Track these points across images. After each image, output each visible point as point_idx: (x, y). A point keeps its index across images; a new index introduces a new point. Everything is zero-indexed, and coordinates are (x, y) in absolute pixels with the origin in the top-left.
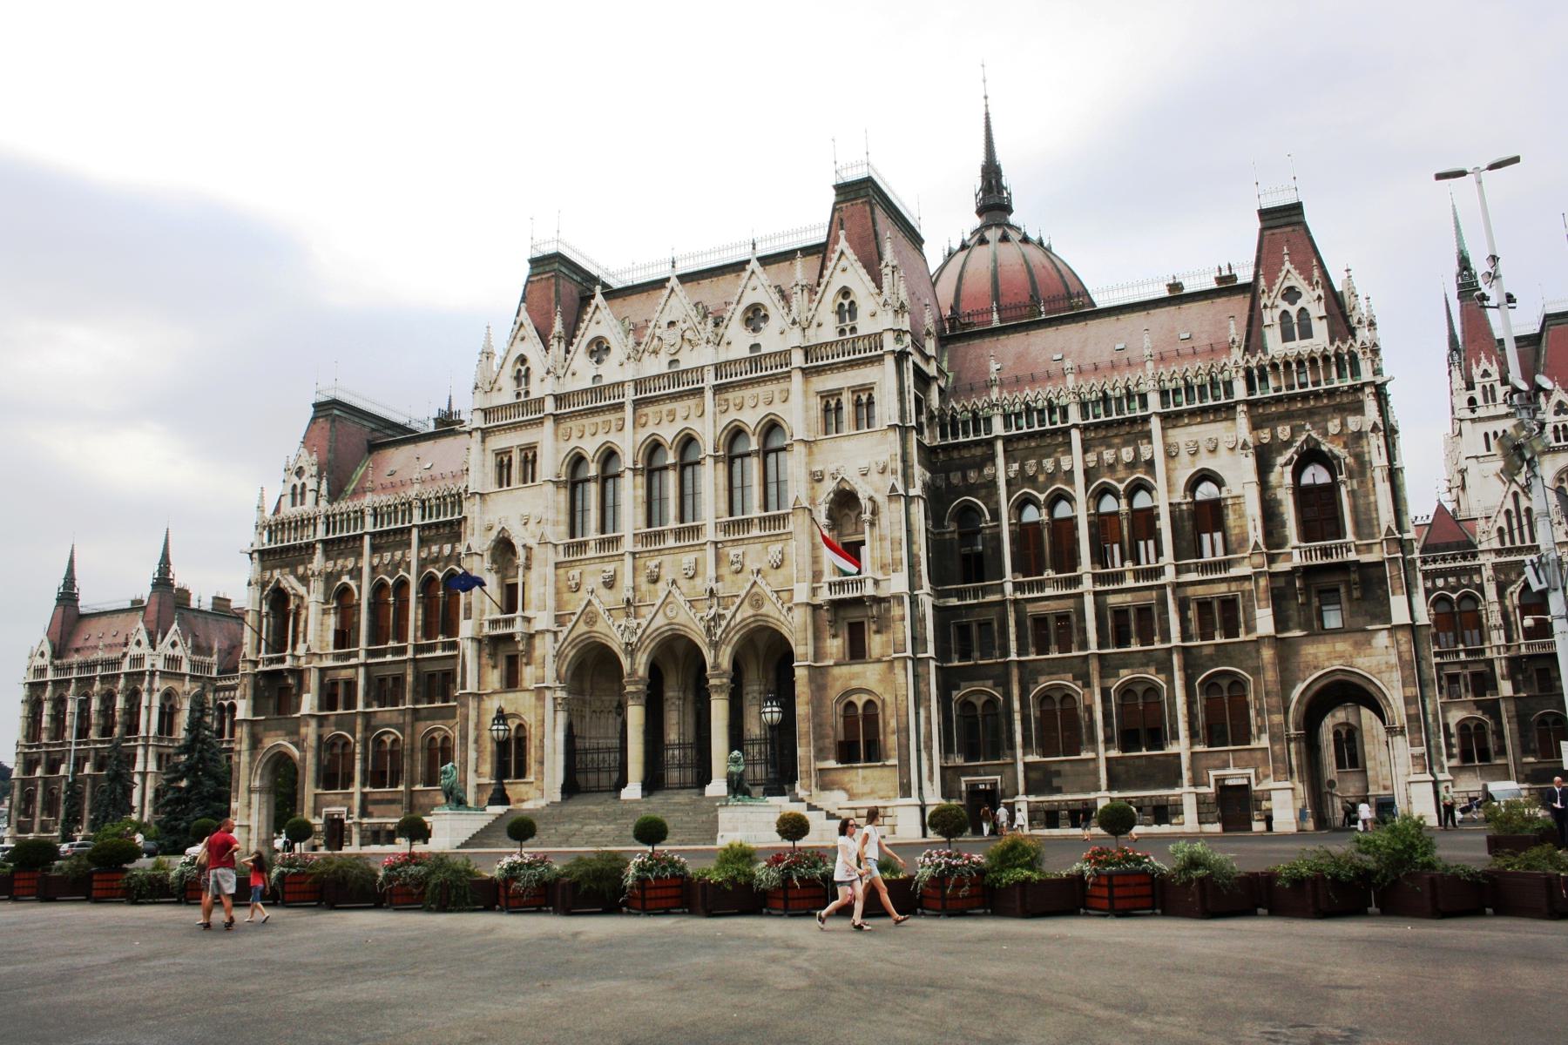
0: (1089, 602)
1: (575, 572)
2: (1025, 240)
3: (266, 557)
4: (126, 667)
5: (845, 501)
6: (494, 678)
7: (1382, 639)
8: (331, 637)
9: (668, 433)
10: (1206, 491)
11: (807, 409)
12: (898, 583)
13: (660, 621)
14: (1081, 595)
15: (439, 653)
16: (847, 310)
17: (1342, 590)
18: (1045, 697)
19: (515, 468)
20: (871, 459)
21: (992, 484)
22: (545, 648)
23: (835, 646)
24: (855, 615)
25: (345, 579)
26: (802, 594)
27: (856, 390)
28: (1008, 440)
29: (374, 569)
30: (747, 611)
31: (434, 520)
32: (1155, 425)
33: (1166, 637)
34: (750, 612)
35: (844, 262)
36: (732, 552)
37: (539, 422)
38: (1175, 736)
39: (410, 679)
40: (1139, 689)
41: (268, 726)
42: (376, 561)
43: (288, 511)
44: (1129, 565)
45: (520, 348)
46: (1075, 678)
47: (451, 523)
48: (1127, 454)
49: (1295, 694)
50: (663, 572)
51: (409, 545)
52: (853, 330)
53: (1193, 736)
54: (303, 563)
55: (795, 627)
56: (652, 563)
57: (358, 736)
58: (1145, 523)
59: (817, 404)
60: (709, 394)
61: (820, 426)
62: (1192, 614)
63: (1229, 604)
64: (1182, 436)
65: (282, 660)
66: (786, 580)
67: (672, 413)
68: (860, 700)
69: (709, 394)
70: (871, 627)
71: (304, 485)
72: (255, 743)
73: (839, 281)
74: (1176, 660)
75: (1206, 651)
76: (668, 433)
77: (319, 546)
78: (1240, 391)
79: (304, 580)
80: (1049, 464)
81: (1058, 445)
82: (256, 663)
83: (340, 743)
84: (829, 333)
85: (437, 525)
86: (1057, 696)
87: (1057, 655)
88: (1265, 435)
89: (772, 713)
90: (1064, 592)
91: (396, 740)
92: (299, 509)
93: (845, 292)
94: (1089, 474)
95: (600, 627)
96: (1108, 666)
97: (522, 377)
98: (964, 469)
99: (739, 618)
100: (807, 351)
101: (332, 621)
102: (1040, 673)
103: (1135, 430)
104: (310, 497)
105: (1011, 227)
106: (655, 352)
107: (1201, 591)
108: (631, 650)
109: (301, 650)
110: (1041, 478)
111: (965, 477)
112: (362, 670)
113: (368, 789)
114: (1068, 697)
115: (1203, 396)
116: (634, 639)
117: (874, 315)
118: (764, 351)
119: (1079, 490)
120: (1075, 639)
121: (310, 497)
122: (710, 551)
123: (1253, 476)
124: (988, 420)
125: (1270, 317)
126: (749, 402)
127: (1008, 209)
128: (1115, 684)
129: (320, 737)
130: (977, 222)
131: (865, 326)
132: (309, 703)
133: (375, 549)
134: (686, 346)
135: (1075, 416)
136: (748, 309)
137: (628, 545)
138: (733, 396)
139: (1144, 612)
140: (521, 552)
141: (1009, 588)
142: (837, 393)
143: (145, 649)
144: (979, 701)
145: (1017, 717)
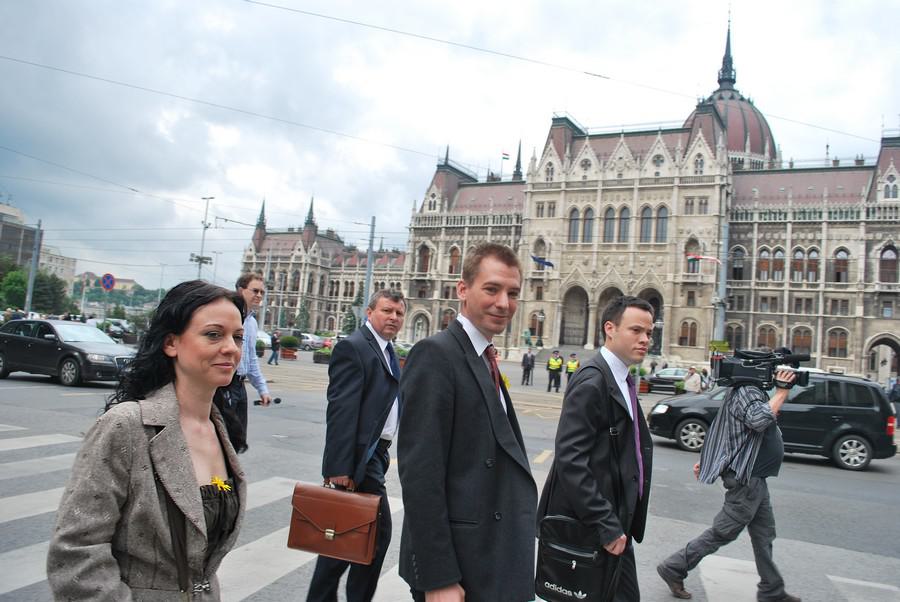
0: (786, 294)
2: (742, 99)
3: (417, 231)
4: (293, 260)
5: (692, 242)
6: (531, 295)
8: (448, 268)
9: (617, 205)
10: (842, 255)
11: (678, 203)
12: (712, 279)
13: (607, 281)
14: (783, 291)
16: (699, 162)
17: (894, 303)
18: (762, 329)
19: (546, 210)
20: (706, 227)
21: (750, 241)
22: (555, 286)
23: (682, 300)
24: (691, 288)
25: (455, 245)
26: (670, 277)
27: (701, 198)
28: (760, 224)
29: (469, 242)
30: (645, 282)
32: (824, 226)
35: (700, 142)
36: (642, 257)
37: (559, 192)
38: (815, 351)
40: (803, 331)
42: (470, 239)
43: (427, 212)
44: (805, 281)
45: (550, 159)
47: (506, 227)
48: (810, 236)
49: (868, 340)
51: (486, 234)
52: (701, 172)
53: (823, 351)
54: (434, 235)
55: (665, 291)
56: (605, 257)
58: (814, 265)
59: (683, 201)
61: (684, 211)
62: (829, 304)
63: (845, 302)
64: (835, 232)
65: (425, 276)
66: (665, 272)
67: (618, 196)
68: (690, 322)
70: (697, 295)
73: (698, 150)
74: (820, 322)
76: (617, 205)
78: (863, 217)
79: (436, 243)
80: (776, 236)
82: (411, 275)
84: (690, 172)
85: (500, 227)
86: (768, 329)
88: (871, 236)
93: (699, 155)
94: (793, 242)
96: (791, 320)
97: (550, 171)
98: (739, 233)
99: (641, 284)
100: (681, 179)
101: (448, 262)
102: (762, 319)
103: (815, 226)
104: (438, 207)
105: (734, 90)
106: (612, 169)
108: (593, 291)
109: (433, 272)
110: (772, 241)
111: (739, 237)
114: (772, 330)
115: (846, 217)
117: (711, 167)
119: (788, 249)
120: (779, 307)
121: (438, 207)
122: (631, 258)
123: (863, 252)
124: (752, 214)
125: (881, 187)
126: (653, 197)
127: (734, 81)
128: (793, 327)
130: (717, 86)
131: (707, 172)
132: (436, 295)
133: (470, 233)
135: (790, 218)
137: (595, 249)
138: (645, 193)
139: (809, 301)
140: (547, 245)
141: (753, 284)
142: (692, 198)
143: (302, 253)
144: (734, 327)
145: (750, 335)
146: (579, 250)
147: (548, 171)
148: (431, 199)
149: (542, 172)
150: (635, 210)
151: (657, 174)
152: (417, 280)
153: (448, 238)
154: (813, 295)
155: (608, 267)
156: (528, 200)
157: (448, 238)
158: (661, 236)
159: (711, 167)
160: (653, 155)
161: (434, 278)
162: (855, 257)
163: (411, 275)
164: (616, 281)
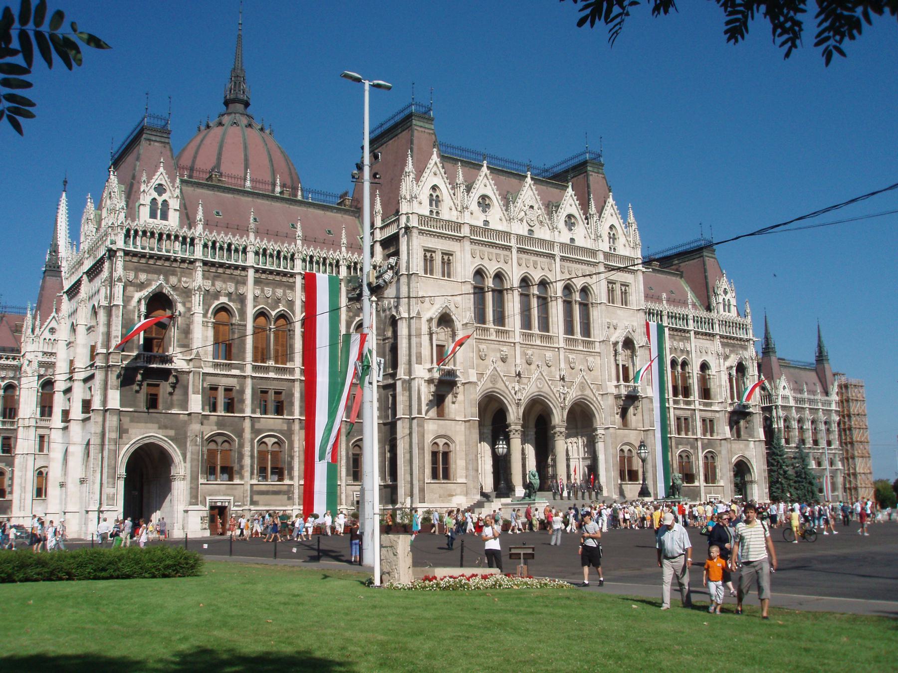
7: (752, 444)
25: (223, 300)
29: (256, 298)
34: (580, 393)
37: (460, 239)
41: (135, 417)
42: (258, 292)
51: (292, 287)
54: (174, 273)
56: (530, 352)
72: (122, 431)
75: (706, 441)
91: (279, 443)
95: (500, 385)
97: (435, 201)
107: (704, 414)
112: (249, 382)
113: (254, 482)
132: (196, 403)
133: (257, 282)
146: (493, 337)
148: (155, 195)
151: (572, 240)
153: (208, 285)
155: (533, 367)
157: (208, 285)
158: (586, 330)
162: (714, 373)
164: (546, 389)
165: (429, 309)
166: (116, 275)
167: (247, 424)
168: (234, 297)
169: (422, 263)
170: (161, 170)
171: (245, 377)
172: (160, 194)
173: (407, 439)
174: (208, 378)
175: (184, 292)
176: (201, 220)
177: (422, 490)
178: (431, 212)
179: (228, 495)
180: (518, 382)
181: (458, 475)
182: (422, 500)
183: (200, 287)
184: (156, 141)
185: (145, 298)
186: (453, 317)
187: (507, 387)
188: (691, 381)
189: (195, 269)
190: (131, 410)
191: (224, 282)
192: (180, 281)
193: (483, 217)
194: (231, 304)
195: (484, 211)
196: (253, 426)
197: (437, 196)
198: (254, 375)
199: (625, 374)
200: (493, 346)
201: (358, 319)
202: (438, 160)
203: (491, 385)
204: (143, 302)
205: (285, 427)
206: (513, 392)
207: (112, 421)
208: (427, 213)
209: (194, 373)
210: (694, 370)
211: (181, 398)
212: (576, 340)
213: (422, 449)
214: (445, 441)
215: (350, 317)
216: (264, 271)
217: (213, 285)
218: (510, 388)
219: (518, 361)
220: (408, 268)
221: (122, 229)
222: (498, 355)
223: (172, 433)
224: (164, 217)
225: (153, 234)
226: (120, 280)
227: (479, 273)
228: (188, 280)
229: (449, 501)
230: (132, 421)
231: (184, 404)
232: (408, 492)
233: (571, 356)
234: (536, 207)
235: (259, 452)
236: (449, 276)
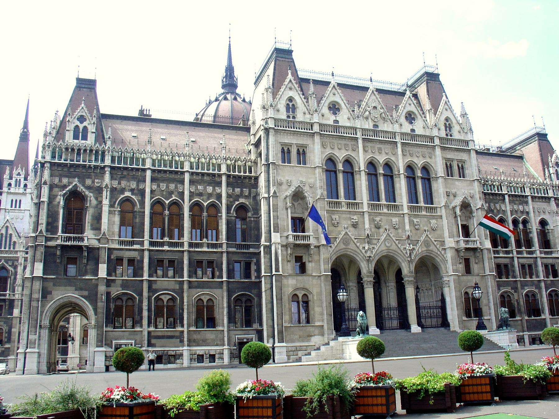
1: (337, 217)
5: (465, 206)
13: (383, 248)
15: (205, 249)
16: (448, 127)
25: (128, 194)
27: (459, 161)
29: (152, 192)
31: (199, 171)
33: (538, 276)
34: (425, 249)
39: (186, 262)
41: (56, 282)
42: (155, 187)
46: (512, 289)
47: (214, 175)
50: (382, 224)
51: (182, 182)
54: (89, 177)
56: (378, 219)
57: (145, 294)
60: (399, 145)
65: (82, 239)
69: (399, 145)
70: (472, 261)
71: (85, 128)
74: (543, 284)
75: (549, 282)
76: (381, 159)
77: (108, 170)
80: (498, 206)
81: (500, 200)
83: (125, 298)
84: (443, 134)
85: (203, 174)
87: (505, 280)
89: (342, 296)
90: (506, 256)
91: (173, 299)
92: (80, 142)
95: (352, 246)
96: (524, 284)
97: (291, 107)
99: (420, 251)
106: (367, 118)
107: (545, 261)
108: (369, 260)
110: (495, 211)
112: (146, 254)
113: (152, 329)
116: (372, 256)
118: (417, 133)
120: (511, 273)
129: (108, 294)
133: (153, 180)
134: (382, 121)
136: (407, 113)
138: (407, 148)
146: (344, 209)
147: (288, 107)
148: (78, 123)
149: (282, 106)
150: (400, 165)
152: (63, 247)
153: (115, 184)
154: (531, 261)
155: (382, 230)
156: (271, 139)
157: (115, 184)
158: (429, 198)
159: (459, 132)
160: (405, 111)
161: (95, 243)
162: (552, 228)
163: (47, 239)
164: (394, 247)
165: (286, 190)
166: (43, 180)
167: (145, 286)
168: (136, 191)
169: (280, 155)
170: (83, 105)
171: (143, 250)
172: (81, 123)
173: (269, 292)
174: (115, 252)
175: (97, 190)
176: (109, 138)
177: (280, 332)
178: (288, 117)
179: (131, 339)
180: (368, 243)
181: (316, 319)
182: (281, 340)
183: (107, 185)
184: (85, 88)
185: (64, 195)
186: (306, 194)
187: (358, 247)
188: (531, 235)
189: (104, 173)
190: (54, 277)
191: (128, 181)
192: (93, 182)
193: (333, 118)
194: (133, 197)
195: (335, 114)
196: (150, 287)
197: (293, 105)
198: (152, 248)
199: (466, 231)
200: (344, 216)
201: (237, 203)
202: (292, 79)
203: (344, 247)
204: (62, 198)
205: (177, 287)
206: (363, 251)
207: (37, 285)
208: (284, 117)
209: (102, 247)
210: (534, 226)
211: (93, 267)
212: (420, 208)
213: (280, 299)
214: (303, 292)
215: (231, 202)
216: (159, 171)
217: (119, 183)
218: (361, 248)
219: (367, 226)
220: (267, 159)
221: (49, 148)
222: (349, 222)
223: (86, 293)
224: (85, 138)
225: (73, 150)
226: (45, 183)
227: (331, 160)
228: (100, 181)
229: (309, 341)
230: (54, 285)
231: (96, 272)
232: (271, 334)
233: (415, 220)
234: (379, 107)
235: (156, 306)
236: (305, 163)
